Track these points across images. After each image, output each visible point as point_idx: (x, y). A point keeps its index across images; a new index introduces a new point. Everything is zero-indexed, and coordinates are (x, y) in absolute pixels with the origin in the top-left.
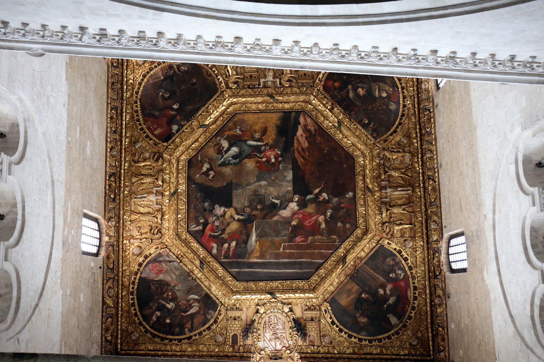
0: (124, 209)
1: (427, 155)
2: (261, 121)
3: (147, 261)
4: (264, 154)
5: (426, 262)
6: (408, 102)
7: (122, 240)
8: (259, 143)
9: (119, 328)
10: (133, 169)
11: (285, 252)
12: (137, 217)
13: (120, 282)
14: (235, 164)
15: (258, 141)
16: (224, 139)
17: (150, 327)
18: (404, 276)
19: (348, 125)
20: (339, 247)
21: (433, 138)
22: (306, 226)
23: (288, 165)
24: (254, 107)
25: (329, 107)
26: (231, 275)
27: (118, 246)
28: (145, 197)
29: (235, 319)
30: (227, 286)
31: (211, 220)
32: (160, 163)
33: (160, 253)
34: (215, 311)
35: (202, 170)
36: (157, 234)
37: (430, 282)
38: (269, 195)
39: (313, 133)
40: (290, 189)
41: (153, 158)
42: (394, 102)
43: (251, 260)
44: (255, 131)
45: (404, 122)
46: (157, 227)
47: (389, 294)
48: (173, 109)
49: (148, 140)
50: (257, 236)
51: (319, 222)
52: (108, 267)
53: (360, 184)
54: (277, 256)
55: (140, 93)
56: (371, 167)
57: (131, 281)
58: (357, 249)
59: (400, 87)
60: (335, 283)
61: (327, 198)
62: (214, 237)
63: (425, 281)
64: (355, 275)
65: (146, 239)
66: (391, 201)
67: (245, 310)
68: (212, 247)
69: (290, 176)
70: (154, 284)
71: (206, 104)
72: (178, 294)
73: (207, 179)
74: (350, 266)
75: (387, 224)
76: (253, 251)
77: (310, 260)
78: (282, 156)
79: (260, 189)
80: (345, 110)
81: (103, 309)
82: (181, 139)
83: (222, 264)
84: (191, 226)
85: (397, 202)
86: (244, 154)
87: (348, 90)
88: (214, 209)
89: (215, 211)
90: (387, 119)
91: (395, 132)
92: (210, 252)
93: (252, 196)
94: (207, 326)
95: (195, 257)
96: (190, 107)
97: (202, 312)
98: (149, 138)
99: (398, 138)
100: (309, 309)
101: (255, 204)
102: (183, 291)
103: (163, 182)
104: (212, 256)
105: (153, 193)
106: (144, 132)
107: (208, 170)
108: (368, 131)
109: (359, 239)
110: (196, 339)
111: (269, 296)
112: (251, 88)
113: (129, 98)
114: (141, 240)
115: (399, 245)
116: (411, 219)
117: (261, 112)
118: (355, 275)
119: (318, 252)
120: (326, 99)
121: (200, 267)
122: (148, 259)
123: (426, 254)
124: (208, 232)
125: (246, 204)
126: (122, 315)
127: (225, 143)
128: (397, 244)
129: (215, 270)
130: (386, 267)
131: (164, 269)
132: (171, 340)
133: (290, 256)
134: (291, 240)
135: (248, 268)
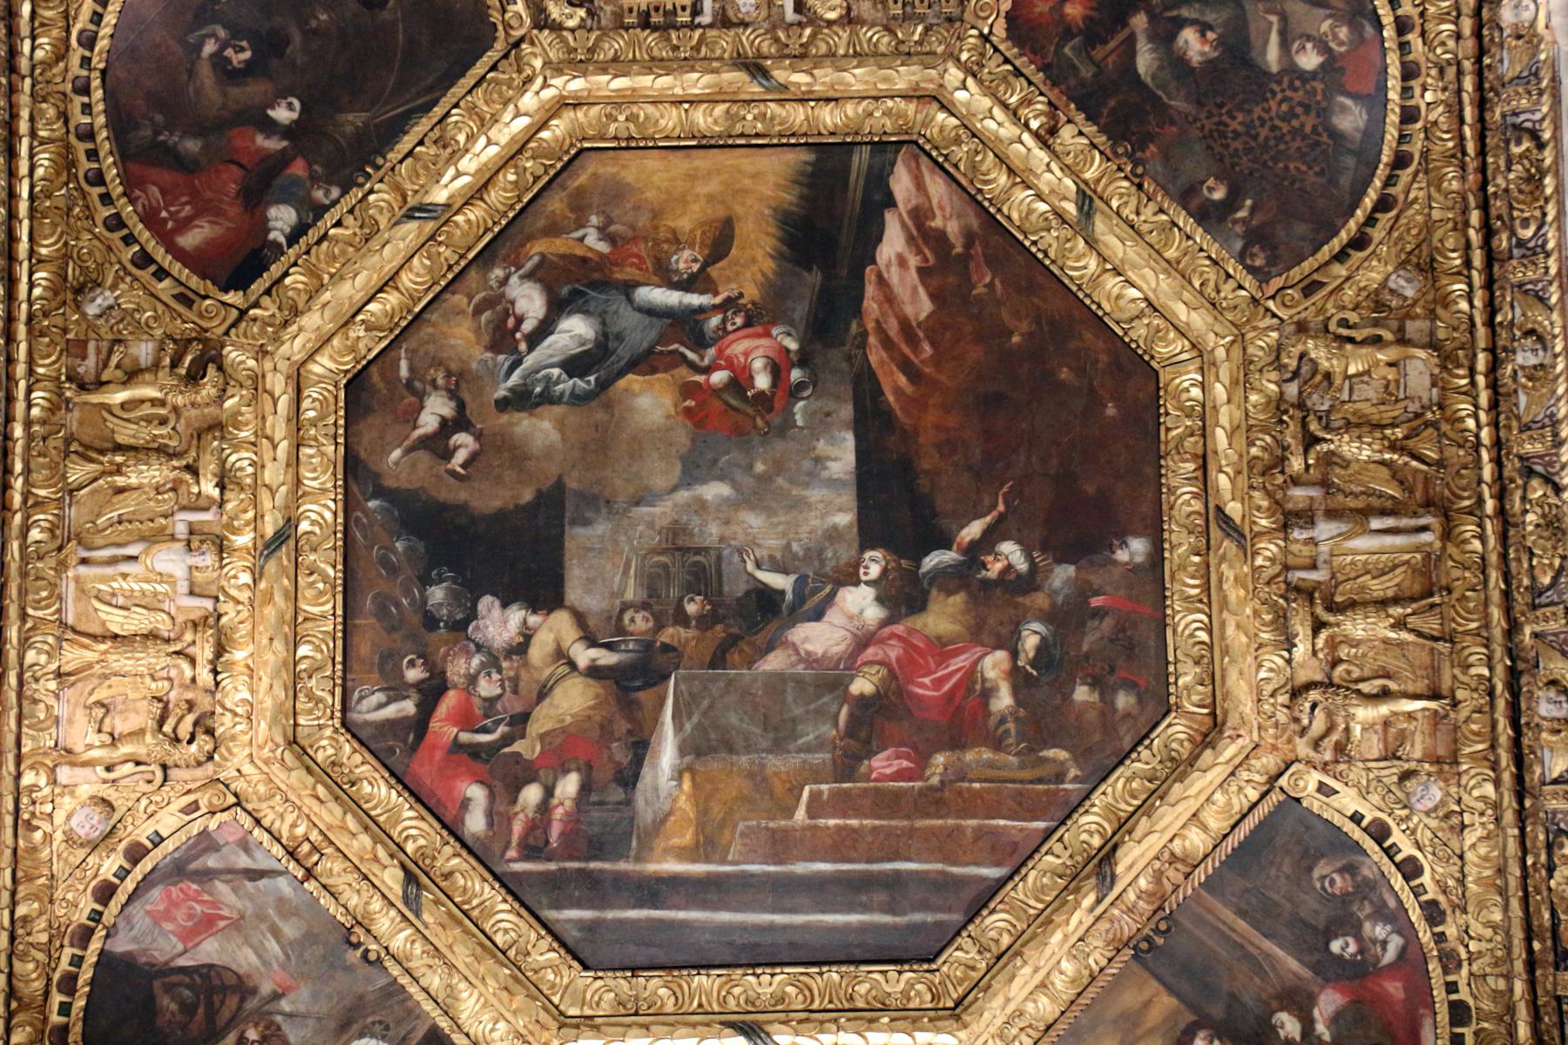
0: (24, 616)
1: (1520, 358)
2: (703, 189)
3: (138, 873)
4: (720, 352)
5: (1513, 883)
6: (1429, 97)
7: (12, 768)
8: (695, 300)
10: (73, 419)
11: (816, 827)
12: (90, 656)
14: (578, 399)
15: (687, 285)
16: (529, 276)
19: (1125, 212)
20: (1080, 805)
21: (1553, 271)
22: (921, 698)
23: (831, 405)
24: (669, 119)
25: (1034, 124)
26: (556, 937)
28: (133, 558)
30: (536, 992)
31: (458, 668)
32: (208, 390)
33: (204, 833)
35: (415, 427)
36: (190, 742)
37: (1532, 984)
39: (959, 249)
40: (844, 519)
41: (175, 364)
42: (1355, 97)
43: (652, 867)
44: (676, 241)
45: (1407, 193)
46: (191, 705)
47: (1327, 1037)
48: (270, 127)
49: (145, 275)
50: (682, 751)
51: (984, 680)
53: (1184, 500)
55: (103, 44)
56: (1238, 414)
57: (56, 977)
58: (1170, 816)
59: (1387, 19)
60: (1059, 982)
61: (1022, 566)
62: (474, 751)
63: (1508, 977)
64: (1160, 941)
65: (138, 763)
66: (1335, 581)
68: (465, 804)
69: (842, 455)
70: (174, 985)
71: (435, 103)
73: (441, 469)
74: (1131, 896)
75: (1314, 695)
76: (663, 821)
77: (939, 866)
78: (804, 360)
79: (696, 520)
80: (1115, 136)
82: (313, 273)
83: (510, 886)
84: (361, 698)
85: (1363, 588)
86: (623, 353)
87: (1131, 40)
88: (472, 615)
89: (477, 628)
90: (1322, 181)
91: (1360, 242)
92: (453, 829)
93: (663, 552)
95: (382, 853)
96: (353, 120)
98: (153, 268)
99: (1372, 275)
101: (674, 593)
102: (319, 1019)
103: (222, 486)
104: (464, 845)
105: (173, 538)
106: (129, 240)
107: (448, 427)
108: (1225, 244)
109: (1180, 767)
112: (655, 28)
113: (48, 65)
114: (109, 769)
115: (1375, 798)
116: (1435, 670)
117: (705, 144)
118: (1160, 941)
119: (979, 829)
120: (1020, 84)
121: (406, 900)
122: (146, 865)
123: (1512, 847)
124: (443, 728)
125: (630, 595)
127: (529, 297)
128: (1364, 794)
129: (475, 913)
130: (1316, 906)
131: (225, 912)
133: (842, 844)
134: (846, 767)
135: (639, 905)
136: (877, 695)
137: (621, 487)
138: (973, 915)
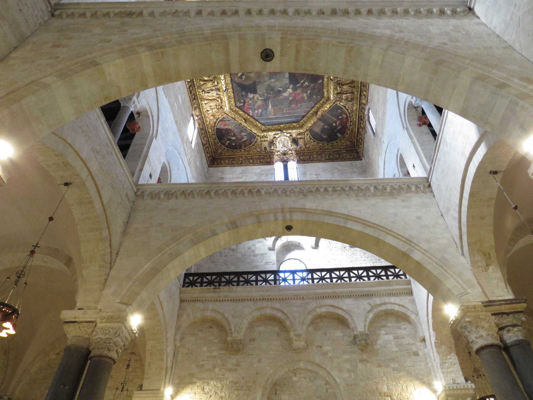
17: (226, 147)
18: (346, 117)
31: (247, 100)
34: (255, 139)
40: (288, 82)
43: (270, 117)
46: (219, 105)
50: (272, 106)
67: (269, 136)
68: (250, 113)
88: (247, 95)
92: (249, 115)
95: (242, 119)
97: (249, 140)
101: (269, 91)
107: (242, 75)
109: (325, 103)
122: (219, 120)
124: (246, 106)
138: (303, 118)
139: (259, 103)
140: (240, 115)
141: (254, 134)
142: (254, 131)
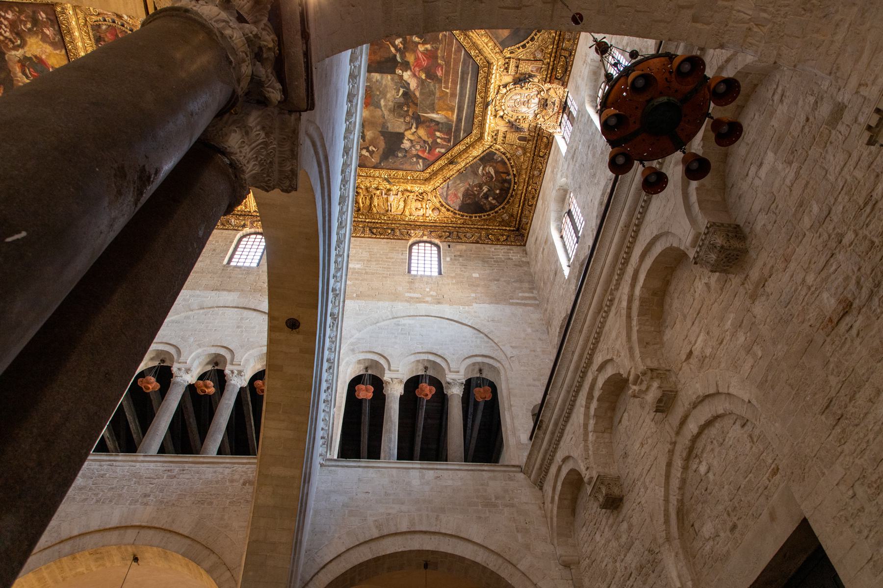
9: (497, 228)
13: (461, 226)
27: (431, 226)
29: (505, 137)
31: (414, 152)
32: (360, 191)
33: (440, 195)
34: (495, 153)
38: (395, 98)
40: (389, 77)
43: (455, 120)
46: (417, 196)
50: (433, 113)
52: (449, 237)
54: (453, 95)
62: (430, 150)
67: (498, 128)
72: (476, 182)
79: (389, 107)
81: (482, 243)
83: (455, 145)
88: (404, 149)
92: (444, 154)
94: (506, 161)
97: (495, 165)
100: (507, 69)
101: (402, 112)
103: (378, 189)
107: (368, 151)
110: (517, 170)
111: (489, 107)
122: (444, 203)
124: (426, 155)
125: (402, 120)
126: (487, 225)
132: (514, 190)
133: (454, 83)
134: (439, 81)
136: (426, 73)
137: (381, 120)
139: (422, 132)
140: (441, 169)
141: (485, 153)
142: (477, 152)
